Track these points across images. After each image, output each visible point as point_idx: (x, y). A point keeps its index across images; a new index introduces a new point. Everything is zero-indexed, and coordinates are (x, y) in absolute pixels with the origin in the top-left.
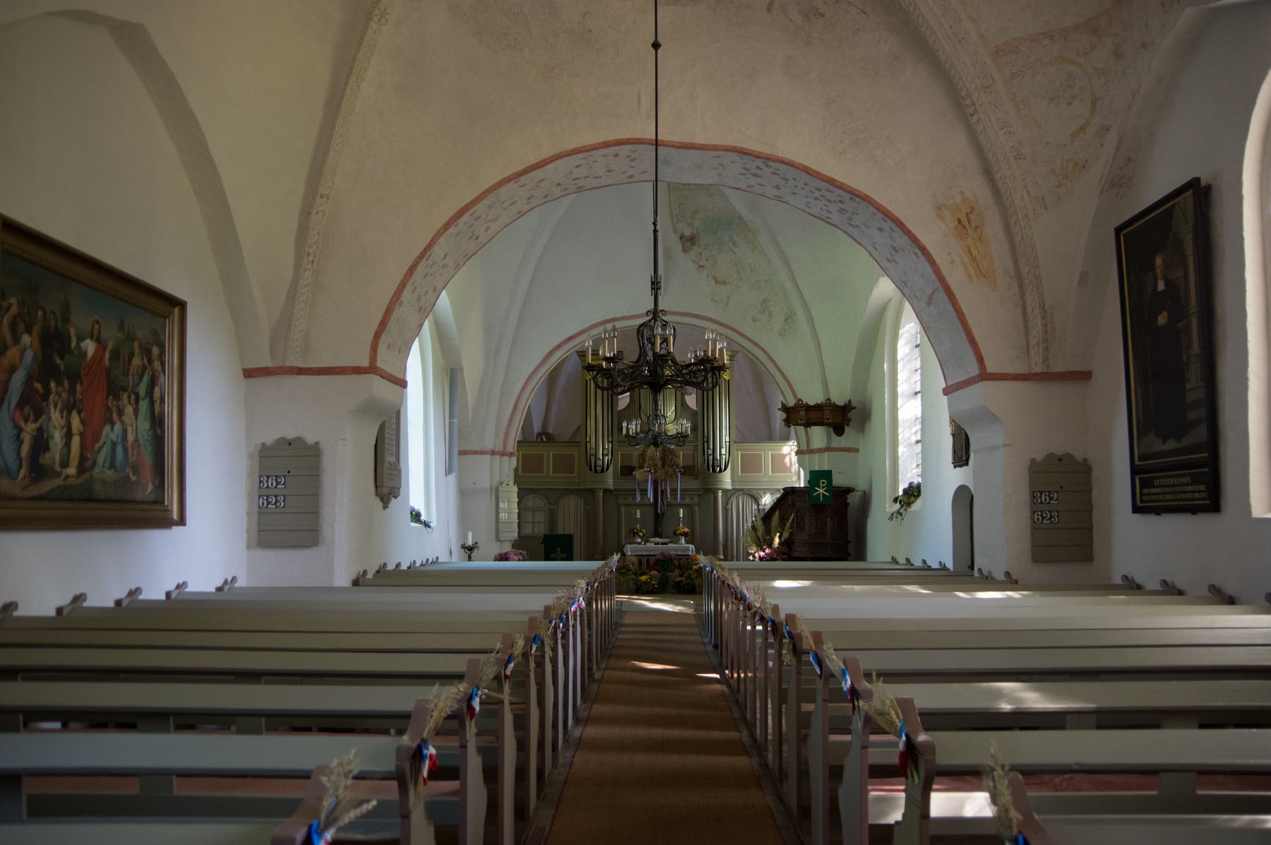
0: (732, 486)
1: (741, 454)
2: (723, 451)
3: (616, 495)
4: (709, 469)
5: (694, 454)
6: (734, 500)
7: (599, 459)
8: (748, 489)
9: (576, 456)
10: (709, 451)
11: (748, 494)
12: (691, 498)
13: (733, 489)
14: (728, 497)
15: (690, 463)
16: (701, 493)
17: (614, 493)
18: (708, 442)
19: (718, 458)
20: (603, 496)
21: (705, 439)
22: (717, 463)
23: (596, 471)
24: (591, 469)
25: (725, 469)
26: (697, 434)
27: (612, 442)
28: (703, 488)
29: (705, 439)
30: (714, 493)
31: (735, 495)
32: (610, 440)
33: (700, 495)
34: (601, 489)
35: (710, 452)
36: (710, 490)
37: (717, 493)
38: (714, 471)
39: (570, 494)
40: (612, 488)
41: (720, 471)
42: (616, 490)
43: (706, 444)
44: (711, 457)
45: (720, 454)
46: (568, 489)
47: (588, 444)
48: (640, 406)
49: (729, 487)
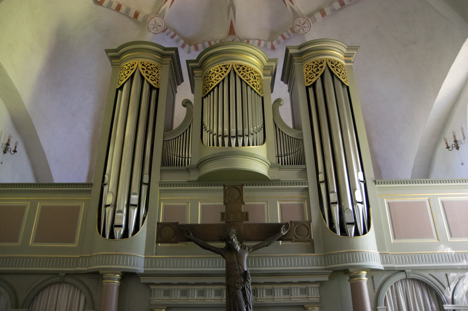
0: (383, 263)
1: (389, 204)
2: (359, 196)
3: (148, 285)
4: (334, 231)
5: (302, 206)
6: (387, 292)
7: (121, 212)
8: (414, 270)
9: (82, 209)
10: (331, 195)
11: (413, 280)
12: (304, 291)
13: (387, 270)
14: (377, 287)
15: (296, 218)
16: (326, 278)
17: (144, 280)
18: (326, 181)
19: (351, 207)
20: (121, 289)
21: (321, 177)
22: (348, 218)
23: (112, 236)
24: (104, 235)
25: (365, 233)
26: (305, 170)
27: (149, 184)
28: (326, 269)
29: (321, 177)
30: (351, 278)
31: (391, 282)
32: (146, 180)
33: (321, 283)
34: (114, 271)
35: (334, 197)
36: (346, 271)
37: (359, 276)
38: (344, 232)
39: (60, 283)
40: (140, 269)
41: (357, 233)
42: (146, 275)
43: (323, 186)
44: (336, 209)
45: (354, 202)
46: (56, 274)
47: (106, 188)
48: (202, 124)
49: (377, 264)
